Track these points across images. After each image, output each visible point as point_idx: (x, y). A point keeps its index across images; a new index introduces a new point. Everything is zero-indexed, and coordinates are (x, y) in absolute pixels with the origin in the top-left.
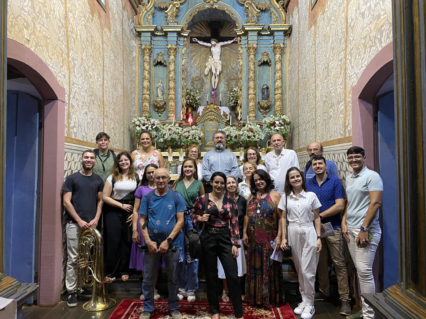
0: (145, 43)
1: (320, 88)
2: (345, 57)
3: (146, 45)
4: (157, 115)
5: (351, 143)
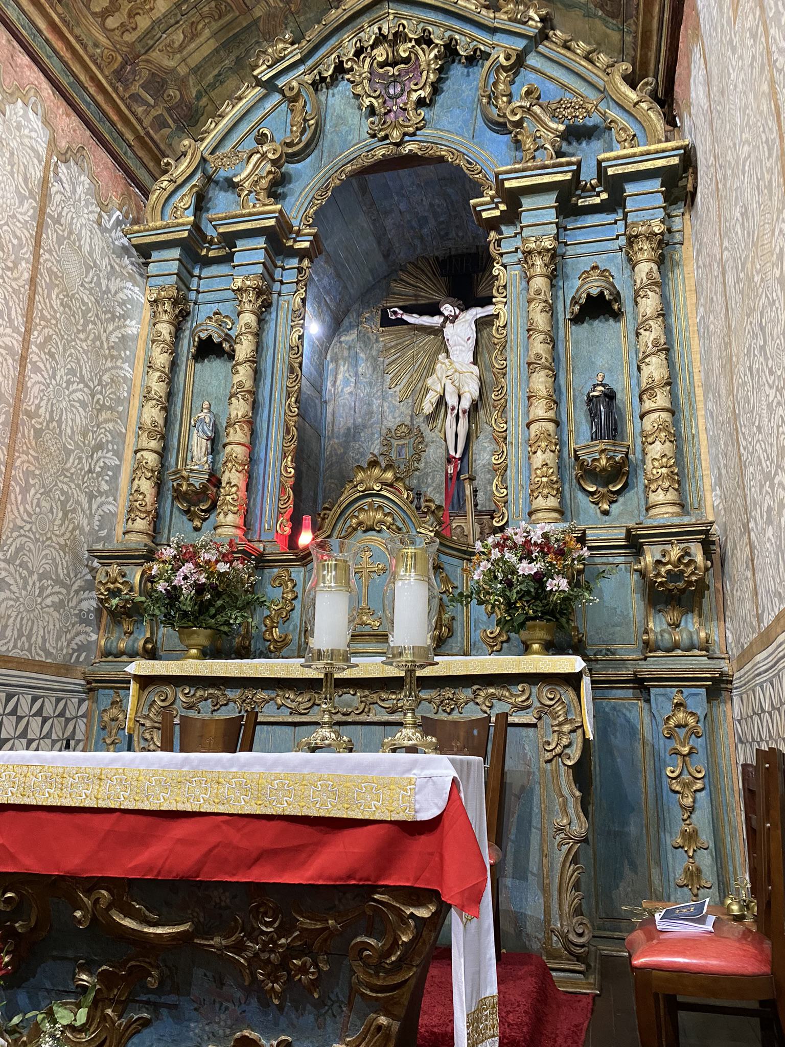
4: (189, 526)
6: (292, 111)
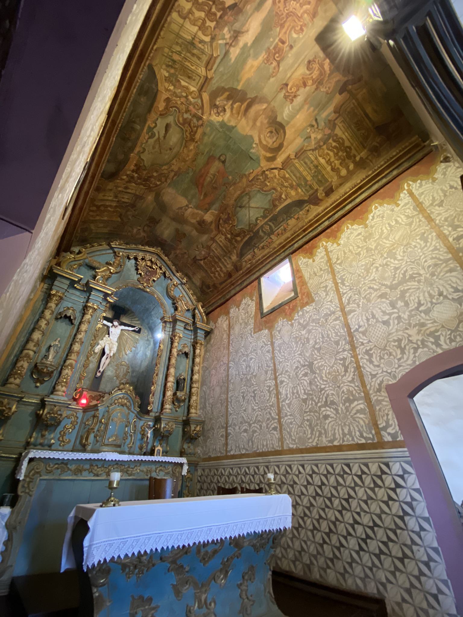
0: (58, 289)
1: (290, 385)
2: (355, 356)
3: (57, 292)
5: (406, 449)
6: (115, 258)
